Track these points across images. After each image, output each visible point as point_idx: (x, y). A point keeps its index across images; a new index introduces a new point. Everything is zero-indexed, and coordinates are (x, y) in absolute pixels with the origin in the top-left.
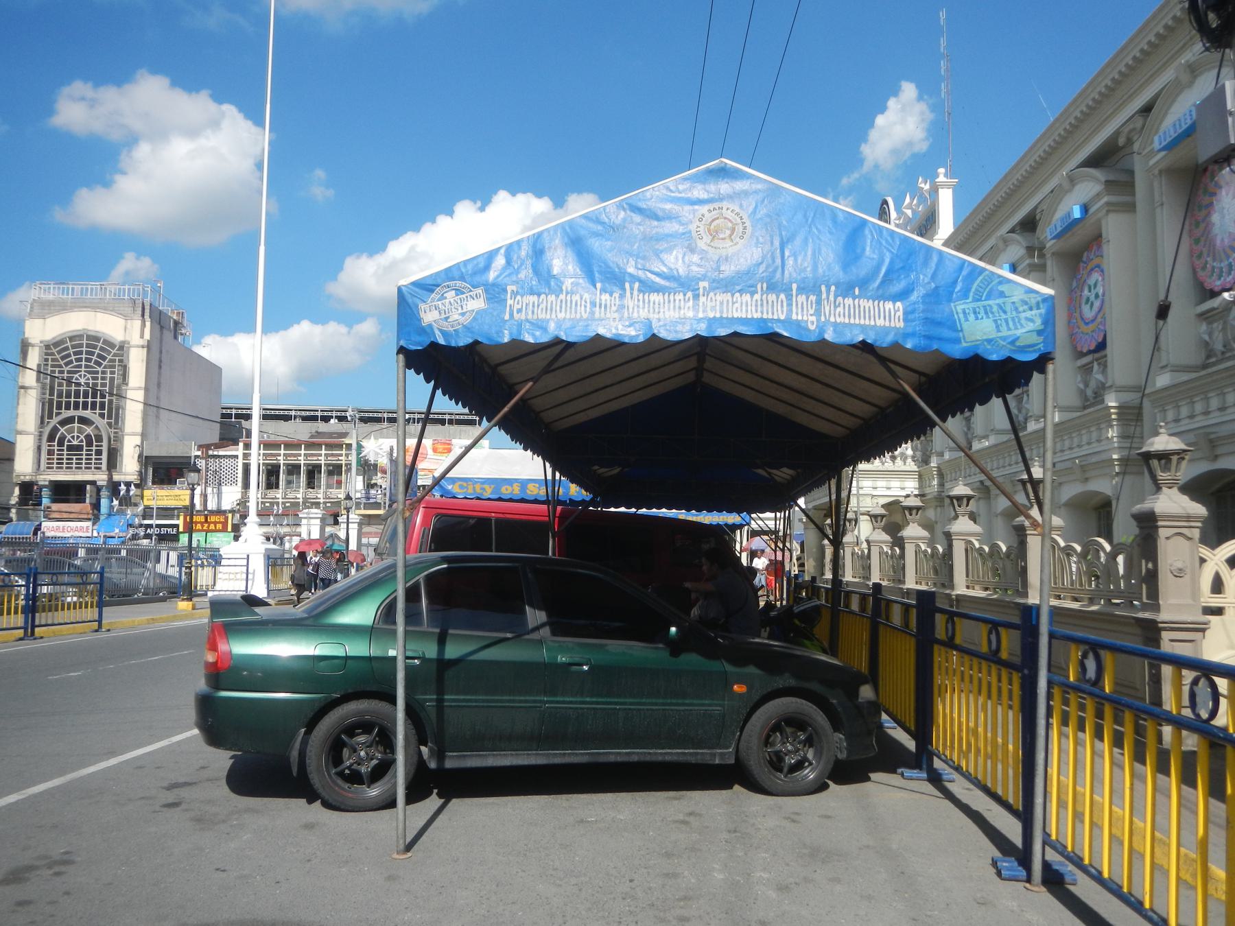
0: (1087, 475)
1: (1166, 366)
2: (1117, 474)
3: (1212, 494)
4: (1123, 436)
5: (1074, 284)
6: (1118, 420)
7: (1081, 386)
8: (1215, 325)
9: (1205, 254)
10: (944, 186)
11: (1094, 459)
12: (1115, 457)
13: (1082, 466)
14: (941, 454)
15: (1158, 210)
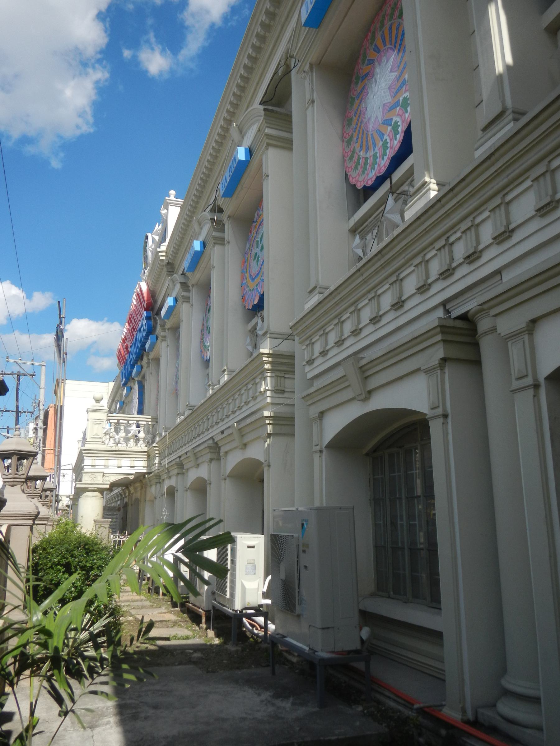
0: (245, 441)
1: (315, 288)
2: (269, 435)
3: (367, 454)
4: (278, 391)
5: (248, 246)
6: (272, 370)
7: (250, 348)
8: (369, 237)
9: (357, 150)
10: (173, 205)
11: (249, 421)
12: (266, 414)
13: (239, 430)
14: (160, 435)
15: (309, 112)
